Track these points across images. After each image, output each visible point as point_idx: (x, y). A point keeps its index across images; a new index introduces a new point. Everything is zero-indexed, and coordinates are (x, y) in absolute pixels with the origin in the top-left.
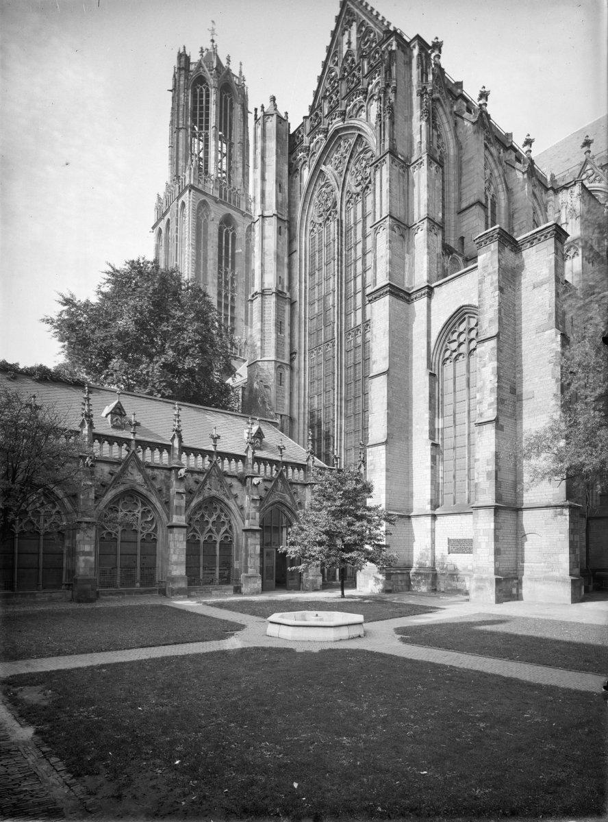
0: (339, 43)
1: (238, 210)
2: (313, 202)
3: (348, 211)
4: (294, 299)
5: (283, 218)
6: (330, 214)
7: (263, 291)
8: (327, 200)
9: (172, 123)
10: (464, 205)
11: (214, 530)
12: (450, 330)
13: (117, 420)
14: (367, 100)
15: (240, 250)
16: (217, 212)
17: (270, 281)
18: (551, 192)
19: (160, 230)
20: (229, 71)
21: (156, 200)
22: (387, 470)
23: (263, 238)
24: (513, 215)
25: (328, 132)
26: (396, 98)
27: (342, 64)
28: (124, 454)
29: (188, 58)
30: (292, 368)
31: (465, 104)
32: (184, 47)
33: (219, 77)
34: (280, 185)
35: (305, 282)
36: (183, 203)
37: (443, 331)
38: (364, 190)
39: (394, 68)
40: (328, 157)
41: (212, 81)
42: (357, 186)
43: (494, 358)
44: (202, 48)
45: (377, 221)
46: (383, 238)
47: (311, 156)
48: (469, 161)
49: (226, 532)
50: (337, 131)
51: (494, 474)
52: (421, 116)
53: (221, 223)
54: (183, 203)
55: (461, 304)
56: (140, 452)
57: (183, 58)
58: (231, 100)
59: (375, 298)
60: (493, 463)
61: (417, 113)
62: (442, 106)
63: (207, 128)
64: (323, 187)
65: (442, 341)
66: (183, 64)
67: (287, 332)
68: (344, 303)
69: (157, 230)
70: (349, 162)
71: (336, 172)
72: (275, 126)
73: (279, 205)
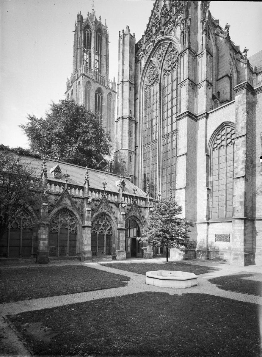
1: (102, 85)
2: (146, 75)
3: (164, 79)
4: (137, 121)
5: (132, 83)
6: (155, 81)
7: (123, 117)
8: (153, 74)
9: (74, 46)
10: (220, 77)
11: (104, 229)
12: (217, 134)
13: (57, 174)
14: (175, 26)
15: (105, 104)
16: (94, 86)
17: (126, 112)
18: (255, 74)
19: (69, 94)
20: (100, 23)
21: (66, 81)
22: (186, 201)
25: (155, 42)
27: (161, 11)
28: (62, 190)
29: (82, 17)
30: (135, 154)
31: (220, 30)
32: (80, 12)
33: (96, 25)
34: (131, 67)
35: (142, 113)
36: (79, 82)
38: (172, 69)
39: (190, 9)
41: (93, 27)
42: (169, 67)
43: (244, 146)
44: (88, 12)
45: (181, 82)
47: (146, 54)
49: (109, 230)
50: (159, 41)
51: (244, 203)
53: (96, 92)
54: (79, 82)
55: (223, 121)
56: (69, 190)
57: (80, 17)
58: (101, 36)
59: (180, 118)
60: (243, 197)
61: (200, 31)
63: (90, 48)
64: (151, 68)
65: (213, 140)
66: (80, 20)
68: (161, 123)
69: (67, 94)
70: (165, 56)
71: (158, 61)
72: (129, 39)
73: (130, 77)
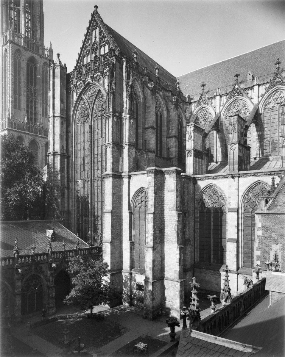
0: (91, 35)
1: (37, 53)
10: (147, 126)
12: (138, 194)
14: (103, 77)
15: (39, 77)
16: (27, 55)
17: (58, 148)
22: (111, 254)
23: (54, 127)
24: (169, 122)
25: (85, 82)
26: (115, 86)
27: (92, 47)
35: (75, 147)
36: (6, 50)
37: (135, 195)
39: (115, 72)
40: (85, 92)
43: (153, 222)
46: (109, 151)
48: (149, 107)
51: (152, 269)
52: (127, 96)
53: (28, 61)
54: (6, 50)
62: (137, 81)
64: (82, 105)
67: (66, 172)
70: (95, 100)
73: (62, 110)
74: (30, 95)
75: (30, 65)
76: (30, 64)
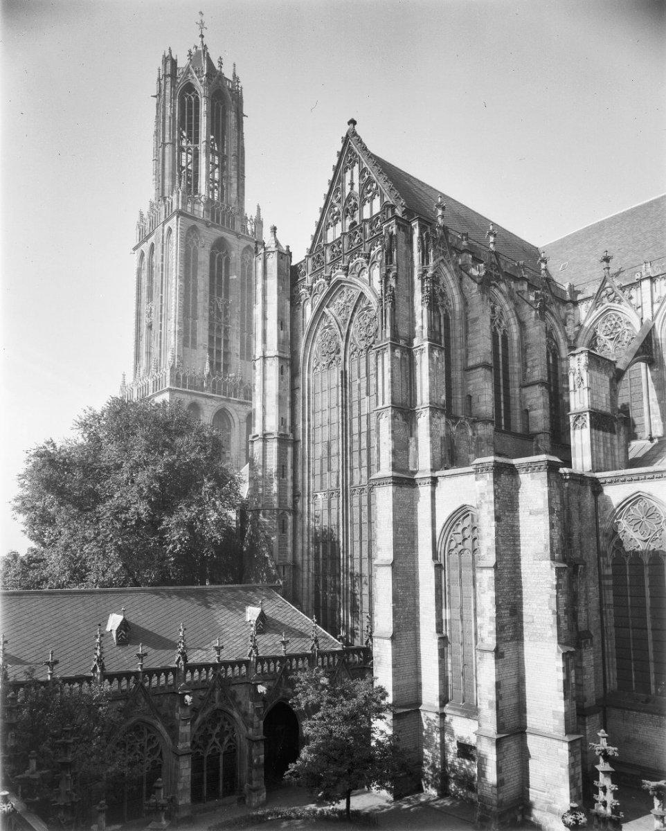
0: (342, 180)
1: (233, 232)
4: (297, 438)
7: (265, 435)
9: (157, 133)
10: (471, 363)
11: (217, 742)
12: (455, 522)
14: (370, 265)
15: (235, 277)
16: (209, 236)
17: (272, 425)
20: (221, 76)
21: (137, 218)
22: (394, 666)
23: (264, 379)
25: (331, 279)
26: (396, 283)
27: (345, 204)
29: (174, 63)
31: (471, 256)
33: (209, 83)
34: (282, 324)
35: (309, 420)
36: (170, 230)
37: (448, 522)
40: (331, 300)
41: (201, 90)
43: (493, 588)
46: (385, 424)
48: (476, 320)
51: (495, 704)
52: (422, 301)
53: (212, 249)
54: (170, 230)
55: (465, 503)
60: (494, 692)
61: (418, 296)
62: (446, 265)
63: (197, 141)
64: (325, 328)
65: (447, 533)
66: (169, 71)
67: (289, 476)
68: (349, 456)
69: (138, 253)
70: (353, 315)
72: (276, 262)
73: (281, 343)
74: (215, 317)
75: (217, 255)
76: (217, 253)
